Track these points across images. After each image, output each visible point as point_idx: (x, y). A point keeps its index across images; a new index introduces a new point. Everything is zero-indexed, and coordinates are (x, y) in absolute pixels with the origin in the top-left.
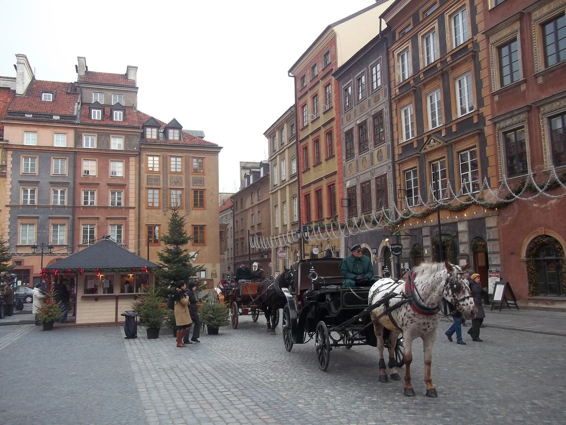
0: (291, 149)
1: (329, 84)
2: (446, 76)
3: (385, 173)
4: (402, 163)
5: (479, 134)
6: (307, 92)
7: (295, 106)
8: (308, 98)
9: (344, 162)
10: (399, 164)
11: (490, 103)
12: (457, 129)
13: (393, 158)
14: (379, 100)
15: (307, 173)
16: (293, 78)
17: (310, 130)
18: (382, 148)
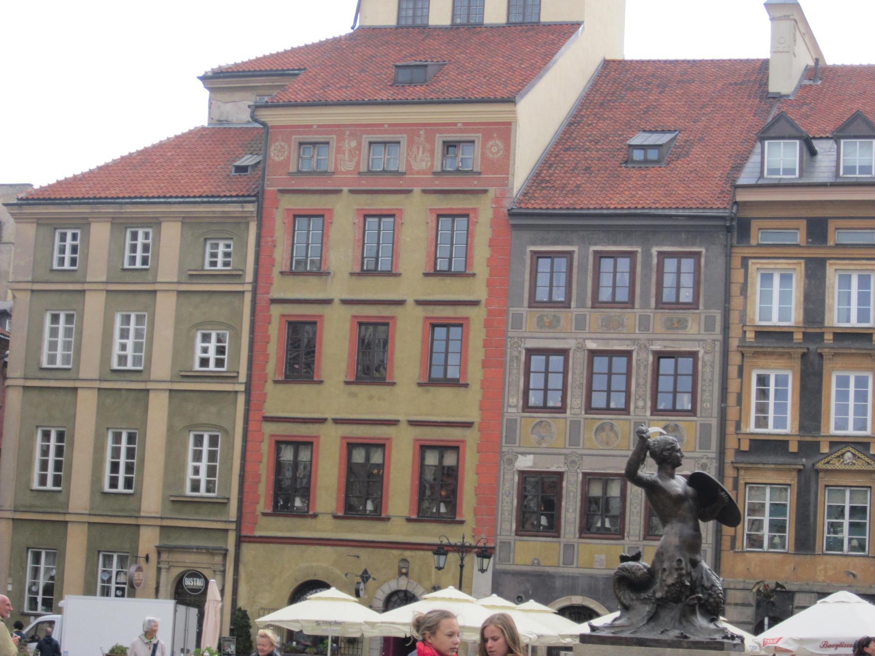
0: (196, 299)
6: (338, 192)
18: (680, 424)
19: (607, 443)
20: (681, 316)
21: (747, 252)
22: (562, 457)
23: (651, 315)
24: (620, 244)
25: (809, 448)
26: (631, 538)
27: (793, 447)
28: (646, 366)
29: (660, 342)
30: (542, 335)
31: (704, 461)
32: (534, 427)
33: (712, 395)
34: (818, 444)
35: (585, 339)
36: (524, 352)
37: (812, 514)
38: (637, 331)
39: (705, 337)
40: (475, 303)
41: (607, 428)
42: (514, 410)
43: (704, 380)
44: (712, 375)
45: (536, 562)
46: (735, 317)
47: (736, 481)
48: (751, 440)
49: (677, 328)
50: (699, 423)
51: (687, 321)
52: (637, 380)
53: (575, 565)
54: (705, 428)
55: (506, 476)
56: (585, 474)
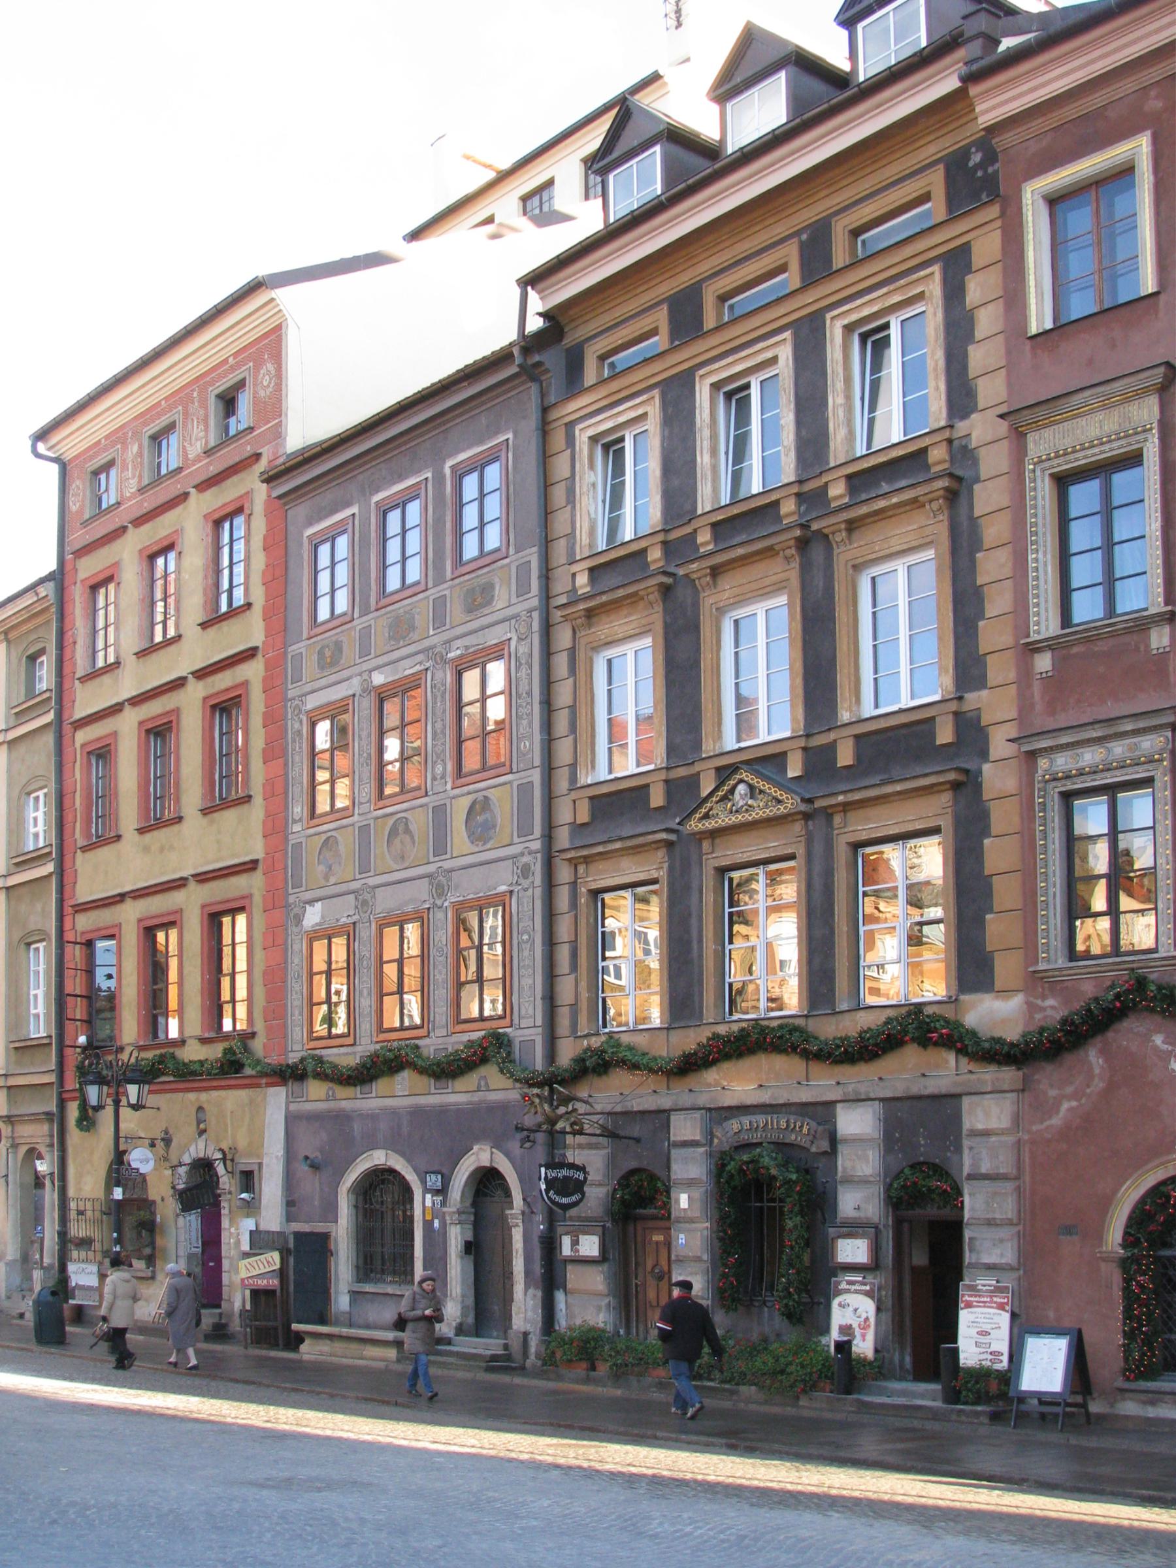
0: (22, 748)
1: (239, 511)
2: (817, 552)
3: (503, 888)
4: (587, 860)
5: (956, 786)
7: (59, 578)
8: (127, 553)
9: (297, 828)
10: (574, 863)
11: (1012, 675)
12: (858, 756)
13: (549, 836)
14: (489, 602)
15: (105, 853)
16: (54, 468)
17: (127, 685)
18: (492, 794)
20: (483, 580)
22: (352, 897)
25: (683, 792)
27: (657, 799)
29: (459, 643)
31: (525, 859)
34: (693, 782)
40: (250, 654)
41: (401, 828)
44: (530, 684)
47: (574, 885)
48: (591, 798)
49: (482, 606)
54: (525, 790)
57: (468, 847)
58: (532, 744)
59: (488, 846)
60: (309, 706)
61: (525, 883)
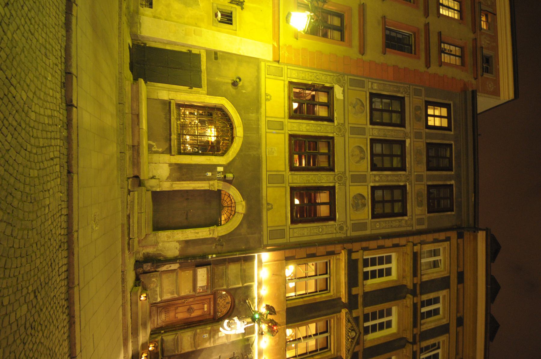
18: (366, 209)
19: (353, 156)
21: (454, 240)
22: (343, 122)
23: (423, 183)
24: (455, 161)
26: (290, 177)
28: (398, 181)
30: (411, 109)
31: (345, 228)
32: (360, 100)
33: (383, 228)
35: (410, 138)
36: (403, 96)
37: (313, 315)
38: (415, 173)
39: (414, 219)
40: (428, 65)
42: (370, 87)
43: (392, 221)
45: (269, 97)
46: (423, 237)
50: (367, 221)
51: (421, 206)
52: (390, 175)
53: (268, 130)
55: (329, 77)
56: (332, 138)
57: (352, 194)
58: (378, 229)
59: (351, 207)
60: (406, 98)
61: (337, 229)
